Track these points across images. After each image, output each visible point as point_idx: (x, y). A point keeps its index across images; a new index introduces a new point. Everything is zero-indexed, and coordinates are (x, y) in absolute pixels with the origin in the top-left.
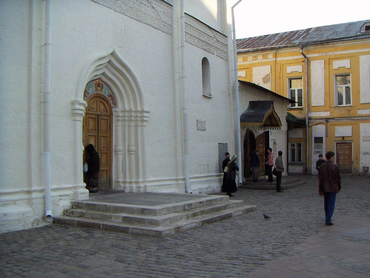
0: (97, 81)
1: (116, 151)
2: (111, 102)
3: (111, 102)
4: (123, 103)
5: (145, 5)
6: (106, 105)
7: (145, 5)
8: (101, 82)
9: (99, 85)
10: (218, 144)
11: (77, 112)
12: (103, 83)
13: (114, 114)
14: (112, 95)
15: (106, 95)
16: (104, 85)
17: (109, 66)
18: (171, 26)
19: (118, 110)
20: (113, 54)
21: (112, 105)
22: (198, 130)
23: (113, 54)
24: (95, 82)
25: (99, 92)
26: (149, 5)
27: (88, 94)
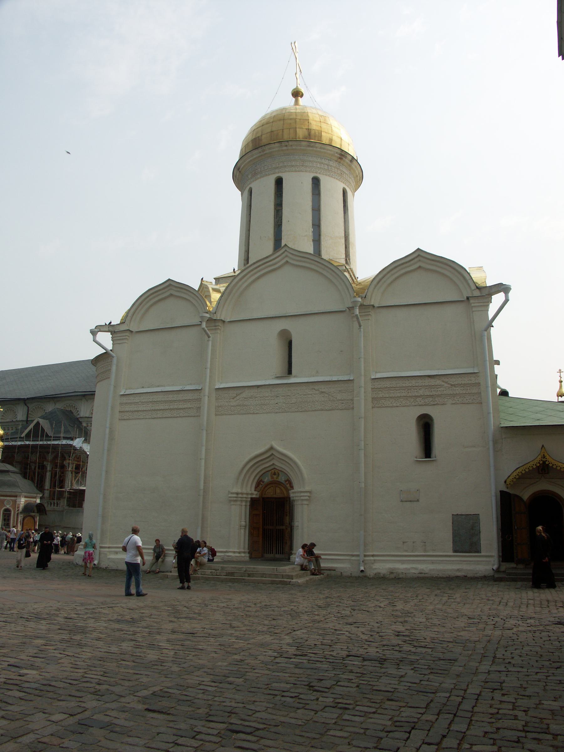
0: (273, 471)
3: (288, 486)
6: (282, 488)
7: (311, 394)
8: (277, 471)
9: (275, 474)
10: (451, 516)
12: (278, 471)
16: (280, 473)
18: (352, 400)
20: (272, 448)
21: (289, 488)
22: (402, 501)
24: (271, 472)
26: (317, 392)
27: (263, 482)
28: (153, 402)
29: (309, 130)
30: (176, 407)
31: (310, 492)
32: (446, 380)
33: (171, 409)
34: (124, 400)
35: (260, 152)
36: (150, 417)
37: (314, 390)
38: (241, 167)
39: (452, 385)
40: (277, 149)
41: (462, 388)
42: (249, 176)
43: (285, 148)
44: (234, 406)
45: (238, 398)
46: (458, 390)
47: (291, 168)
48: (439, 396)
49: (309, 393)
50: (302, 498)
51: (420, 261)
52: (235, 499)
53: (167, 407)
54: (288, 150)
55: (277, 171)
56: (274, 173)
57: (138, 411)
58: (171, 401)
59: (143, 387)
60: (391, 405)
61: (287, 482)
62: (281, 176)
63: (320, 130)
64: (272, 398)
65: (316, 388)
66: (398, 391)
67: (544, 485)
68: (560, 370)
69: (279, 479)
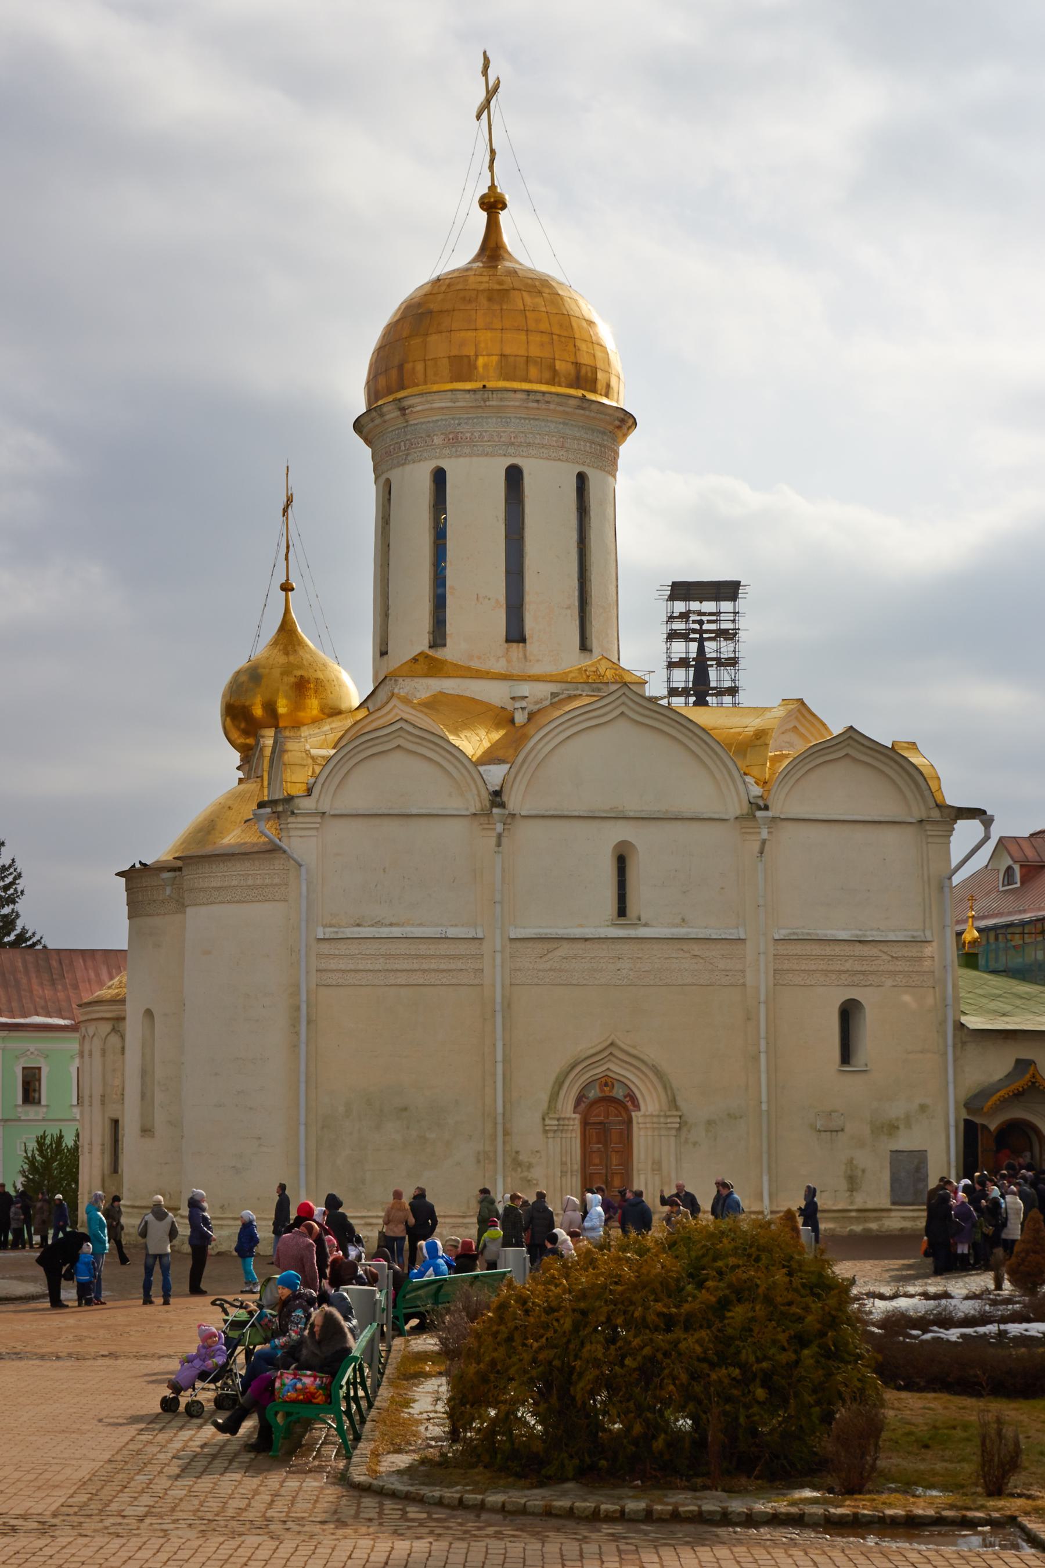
1: (638, 1171)
2: (629, 1104)
3: (629, 1104)
4: (646, 1105)
5: (676, 958)
7: (676, 958)
8: (610, 1079)
9: (606, 1084)
11: (547, 1128)
15: (621, 1098)
16: (616, 1084)
17: (614, 1059)
18: (743, 971)
21: (631, 1108)
23: (612, 1044)
25: (608, 1094)
26: (687, 955)
27: (587, 1098)
28: (388, 956)
29: (577, 365)
30: (433, 966)
32: (885, 949)
33: (424, 971)
34: (325, 948)
35: (476, 400)
36: (382, 983)
37: (681, 952)
38: (415, 410)
39: (892, 957)
40: (517, 404)
41: (908, 963)
42: (437, 440)
43: (535, 405)
44: (542, 971)
45: (550, 955)
46: (901, 966)
47: (541, 451)
48: (872, 972)
49: (673, 956)
50: (669, 1125)
51: (848, 745)
52: (556, 1128)
53: (416, 966)
54: (539, 409)
55: (511, 450)
56: (505, 455)
57: (356, 971)
58: (417, 956)
59: (358, 925)
60: (802, 983)
61: (628, 1099)
63: (592, 364)
64: (611, 961)
65: (685, 948)
66: (813, 962)
67: (1018, 1113)
69: (614, 1094)
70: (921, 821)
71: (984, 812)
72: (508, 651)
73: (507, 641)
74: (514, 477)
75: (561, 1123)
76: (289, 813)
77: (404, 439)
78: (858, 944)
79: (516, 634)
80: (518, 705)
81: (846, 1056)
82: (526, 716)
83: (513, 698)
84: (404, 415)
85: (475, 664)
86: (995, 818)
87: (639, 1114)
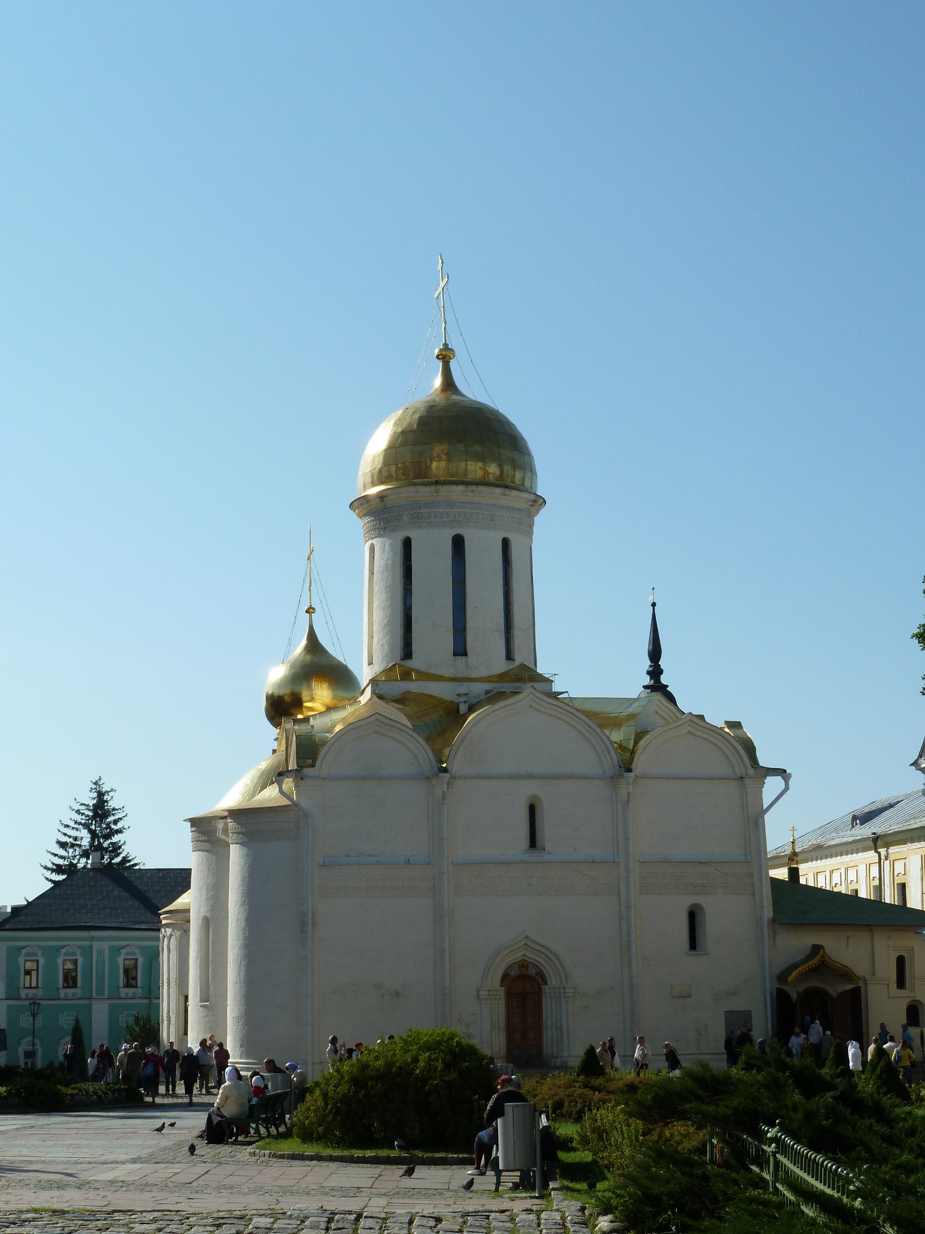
3: (540, 979)
8: (526, 962)
12: (527, 963)
13: (543, 990)
14: (541, 972)
19: (546, 989)
20: (527, 937)
21: (541, 982)
22: (674, 997)
27: (510, 976)
31: (575, 988)
39: (724, 874)
59: (348, 856)
62: (462, 534)
67: (815, 983)
68: (793, 827)
70: (742, 778)
71: (785, 771)
72: (455, 661)
73: (455, 655)
74: (458, 543)
75: (491, 993)
76: (300, 779)
77: (383, 517)
78: (698, 864)
79: (460, 650)
80: (462, 699)
81: (693, 944)
82: (467, 707)
83: (459, 695)
84: (383, 501)
85: (433, 671)
86: (792, 775)
87: (546, 987)
